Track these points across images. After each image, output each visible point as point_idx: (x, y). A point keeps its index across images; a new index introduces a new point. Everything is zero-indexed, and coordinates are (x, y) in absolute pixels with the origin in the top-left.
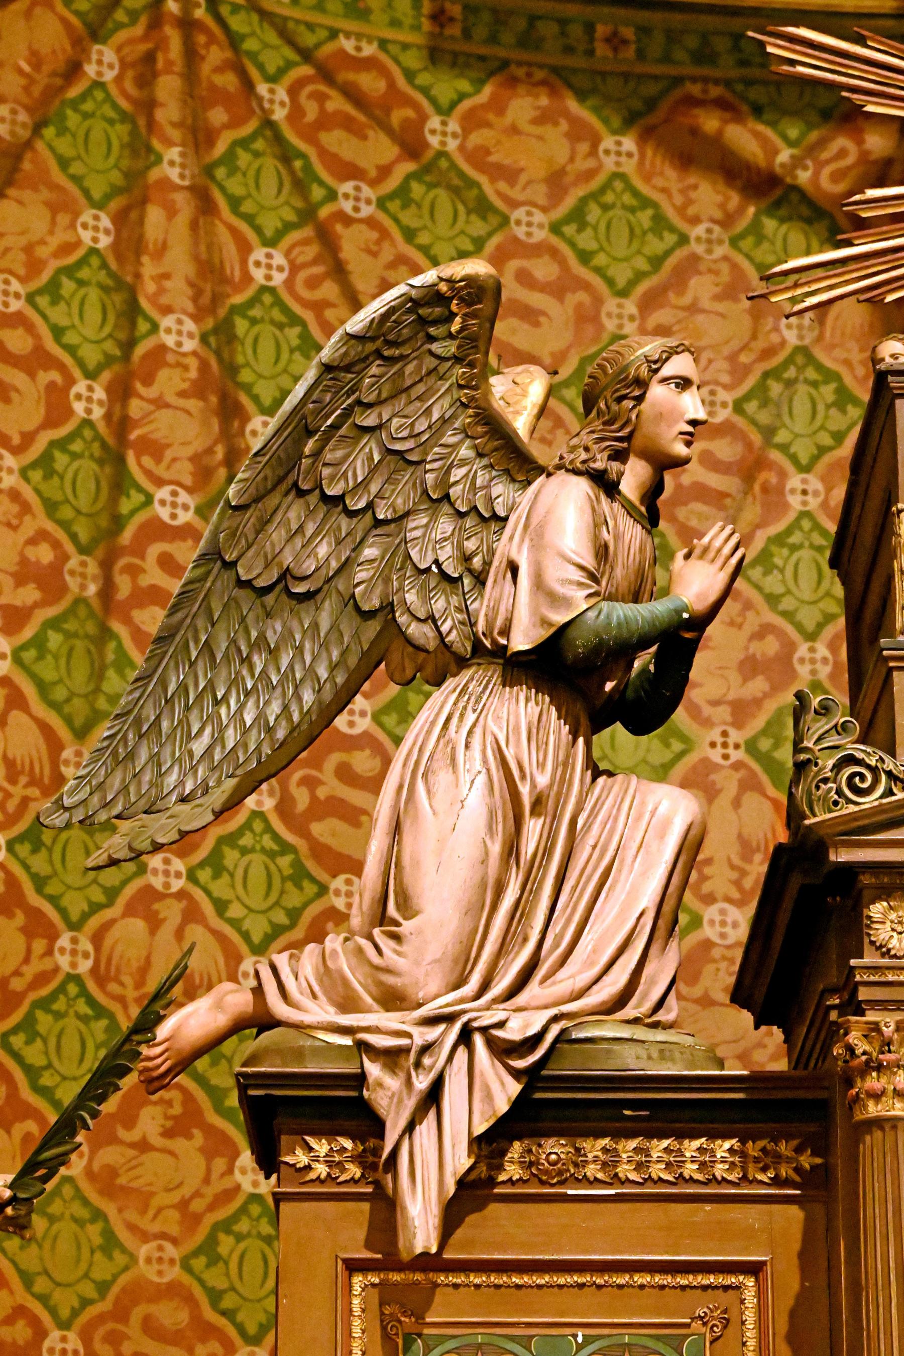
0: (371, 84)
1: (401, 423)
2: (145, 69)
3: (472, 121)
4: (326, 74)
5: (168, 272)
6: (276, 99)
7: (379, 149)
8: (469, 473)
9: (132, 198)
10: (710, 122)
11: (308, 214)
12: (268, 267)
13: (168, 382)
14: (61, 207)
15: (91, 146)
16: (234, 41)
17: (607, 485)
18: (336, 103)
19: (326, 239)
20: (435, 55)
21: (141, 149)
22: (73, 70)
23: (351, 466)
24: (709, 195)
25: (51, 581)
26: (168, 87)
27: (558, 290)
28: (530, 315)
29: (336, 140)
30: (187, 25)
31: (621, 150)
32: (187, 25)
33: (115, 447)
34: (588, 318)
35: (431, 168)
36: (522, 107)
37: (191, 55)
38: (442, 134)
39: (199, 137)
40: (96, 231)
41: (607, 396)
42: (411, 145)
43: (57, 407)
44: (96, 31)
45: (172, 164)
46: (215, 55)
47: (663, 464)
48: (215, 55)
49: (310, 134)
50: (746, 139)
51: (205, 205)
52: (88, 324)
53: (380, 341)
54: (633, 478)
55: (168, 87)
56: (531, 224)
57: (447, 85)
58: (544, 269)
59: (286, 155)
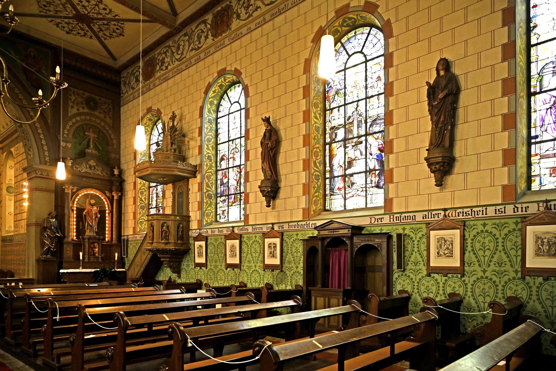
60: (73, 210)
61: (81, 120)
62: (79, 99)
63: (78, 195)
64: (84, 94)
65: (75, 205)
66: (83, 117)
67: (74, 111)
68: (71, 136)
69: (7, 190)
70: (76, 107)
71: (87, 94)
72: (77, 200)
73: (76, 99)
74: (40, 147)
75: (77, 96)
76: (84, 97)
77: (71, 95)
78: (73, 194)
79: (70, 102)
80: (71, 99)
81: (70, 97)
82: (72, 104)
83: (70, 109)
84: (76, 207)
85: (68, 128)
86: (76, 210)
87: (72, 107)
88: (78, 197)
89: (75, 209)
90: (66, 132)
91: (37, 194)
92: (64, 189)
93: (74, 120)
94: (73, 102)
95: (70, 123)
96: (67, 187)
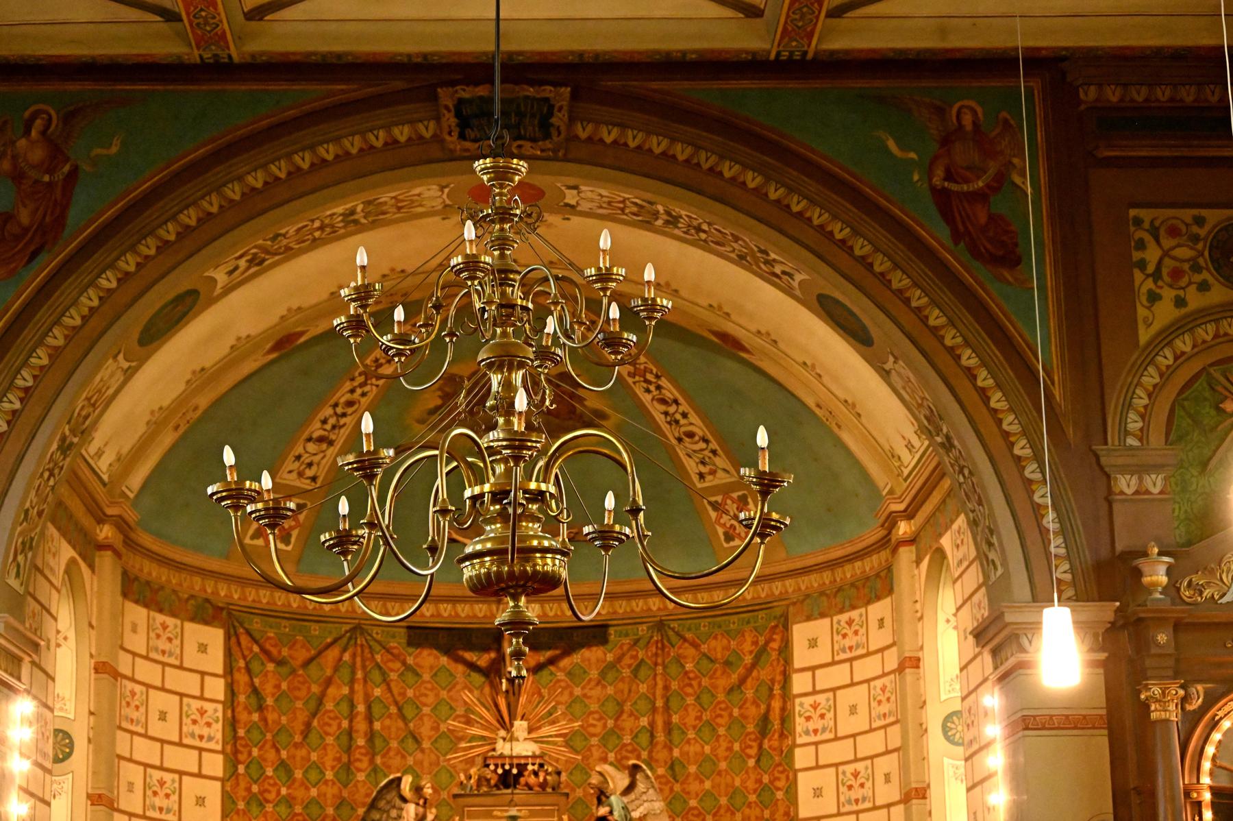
0: (395, 651)
1: (389, 797)
2: (354, 656)
3: (416, 657)
4: (388, 651)
5: (359, 697)
6: (378, 658)
7: (397, 665)
8: (398, 802)
9: (352, 681)
10: (461, 653)
11: (385, 680)
12: (377, 692)
13: (360, 718)
14: (339, 687)
15: (345, 673)
16: (370, 647)
17: (417, 804)
18: (390, 657)
19: (388, 685)
20: (410, 644)
21: (353, 672)
22: (341, 659)
23: (382, 804)
24: (461, 668)
25: (339, 759)
26: (358, 659)
27: (431, 690)
28: (426, 695)
29: (391, 665)
30: (362, 646)
31: (444, 660)
32: (362, 646)
33: (350, 733)
34: (437, 695)
35: (408, 668)
36: (426, 652)
37: (363, 652)
38: (410, 660)
39: (364, 667)
40: (346, 690)
41: (418, 790)
42: (404, 663)
43: (339, 726)
44: (344, 650)
45: (359, 675)
46: (367, 651)
47: (426, 800)
48: (367, 651)
49: (385, 663)
50: (468, 656)
51: (365, 681)
52: (344, 707)
53: (386, 786)
54: (421, 802)
55: (358, 659)
56: (426, 677)
57: (411, 650)
58: (429, 686)
59: (380, 668)
60: (1198, 805)
61: (1201, 348)
62: (1184, 252)
63: (1214, 725)
64: (1200, 221)
65: (1206, 780)
66: (1206, 333)
67: (1165, 312)
68: (1156, 438)
69: (945, 730)
70: (1168, 294)
71: (1214, 217)
72: (1210, 750)
73: (1166, 254)
74: (1028, 521)
75: (1167, 243)
76: (1203, 232)
77: (1141, 245)
78: (1192, 720)
79: (1138, 275)
80: (1142, 265)
81: (1137, 256)
82: (1149, 284)
83: (1142, 312)
84: (1215, 791)
85: (1141, 400)
86: (1214, 806)
87: (1154, 298)
88: (1216, 736)
89: (1207, 796)
90: (1134, 423)
91: (1040, 742)
92: (1145, 706)
93: (1166, 359)
94: (1157, 275)
95: (1151, 378)
96: (1156, 690)
